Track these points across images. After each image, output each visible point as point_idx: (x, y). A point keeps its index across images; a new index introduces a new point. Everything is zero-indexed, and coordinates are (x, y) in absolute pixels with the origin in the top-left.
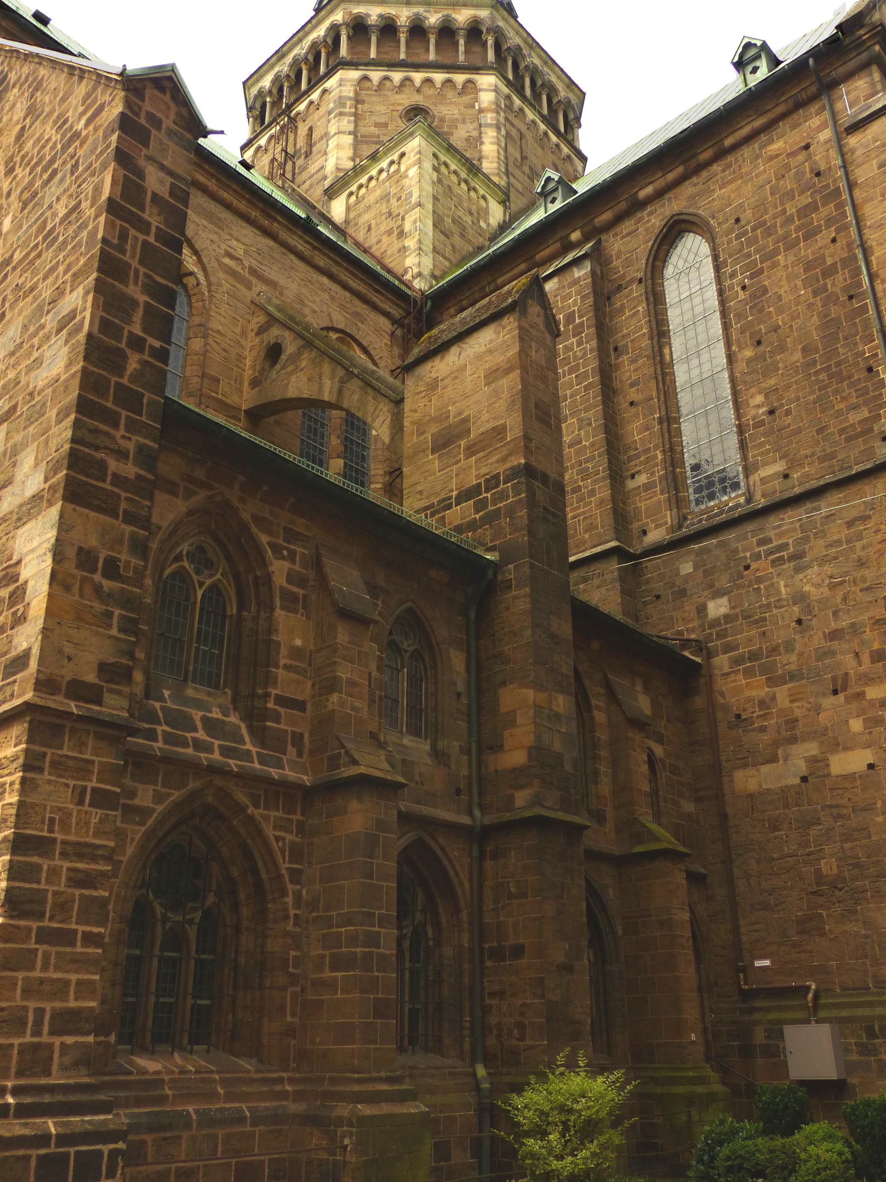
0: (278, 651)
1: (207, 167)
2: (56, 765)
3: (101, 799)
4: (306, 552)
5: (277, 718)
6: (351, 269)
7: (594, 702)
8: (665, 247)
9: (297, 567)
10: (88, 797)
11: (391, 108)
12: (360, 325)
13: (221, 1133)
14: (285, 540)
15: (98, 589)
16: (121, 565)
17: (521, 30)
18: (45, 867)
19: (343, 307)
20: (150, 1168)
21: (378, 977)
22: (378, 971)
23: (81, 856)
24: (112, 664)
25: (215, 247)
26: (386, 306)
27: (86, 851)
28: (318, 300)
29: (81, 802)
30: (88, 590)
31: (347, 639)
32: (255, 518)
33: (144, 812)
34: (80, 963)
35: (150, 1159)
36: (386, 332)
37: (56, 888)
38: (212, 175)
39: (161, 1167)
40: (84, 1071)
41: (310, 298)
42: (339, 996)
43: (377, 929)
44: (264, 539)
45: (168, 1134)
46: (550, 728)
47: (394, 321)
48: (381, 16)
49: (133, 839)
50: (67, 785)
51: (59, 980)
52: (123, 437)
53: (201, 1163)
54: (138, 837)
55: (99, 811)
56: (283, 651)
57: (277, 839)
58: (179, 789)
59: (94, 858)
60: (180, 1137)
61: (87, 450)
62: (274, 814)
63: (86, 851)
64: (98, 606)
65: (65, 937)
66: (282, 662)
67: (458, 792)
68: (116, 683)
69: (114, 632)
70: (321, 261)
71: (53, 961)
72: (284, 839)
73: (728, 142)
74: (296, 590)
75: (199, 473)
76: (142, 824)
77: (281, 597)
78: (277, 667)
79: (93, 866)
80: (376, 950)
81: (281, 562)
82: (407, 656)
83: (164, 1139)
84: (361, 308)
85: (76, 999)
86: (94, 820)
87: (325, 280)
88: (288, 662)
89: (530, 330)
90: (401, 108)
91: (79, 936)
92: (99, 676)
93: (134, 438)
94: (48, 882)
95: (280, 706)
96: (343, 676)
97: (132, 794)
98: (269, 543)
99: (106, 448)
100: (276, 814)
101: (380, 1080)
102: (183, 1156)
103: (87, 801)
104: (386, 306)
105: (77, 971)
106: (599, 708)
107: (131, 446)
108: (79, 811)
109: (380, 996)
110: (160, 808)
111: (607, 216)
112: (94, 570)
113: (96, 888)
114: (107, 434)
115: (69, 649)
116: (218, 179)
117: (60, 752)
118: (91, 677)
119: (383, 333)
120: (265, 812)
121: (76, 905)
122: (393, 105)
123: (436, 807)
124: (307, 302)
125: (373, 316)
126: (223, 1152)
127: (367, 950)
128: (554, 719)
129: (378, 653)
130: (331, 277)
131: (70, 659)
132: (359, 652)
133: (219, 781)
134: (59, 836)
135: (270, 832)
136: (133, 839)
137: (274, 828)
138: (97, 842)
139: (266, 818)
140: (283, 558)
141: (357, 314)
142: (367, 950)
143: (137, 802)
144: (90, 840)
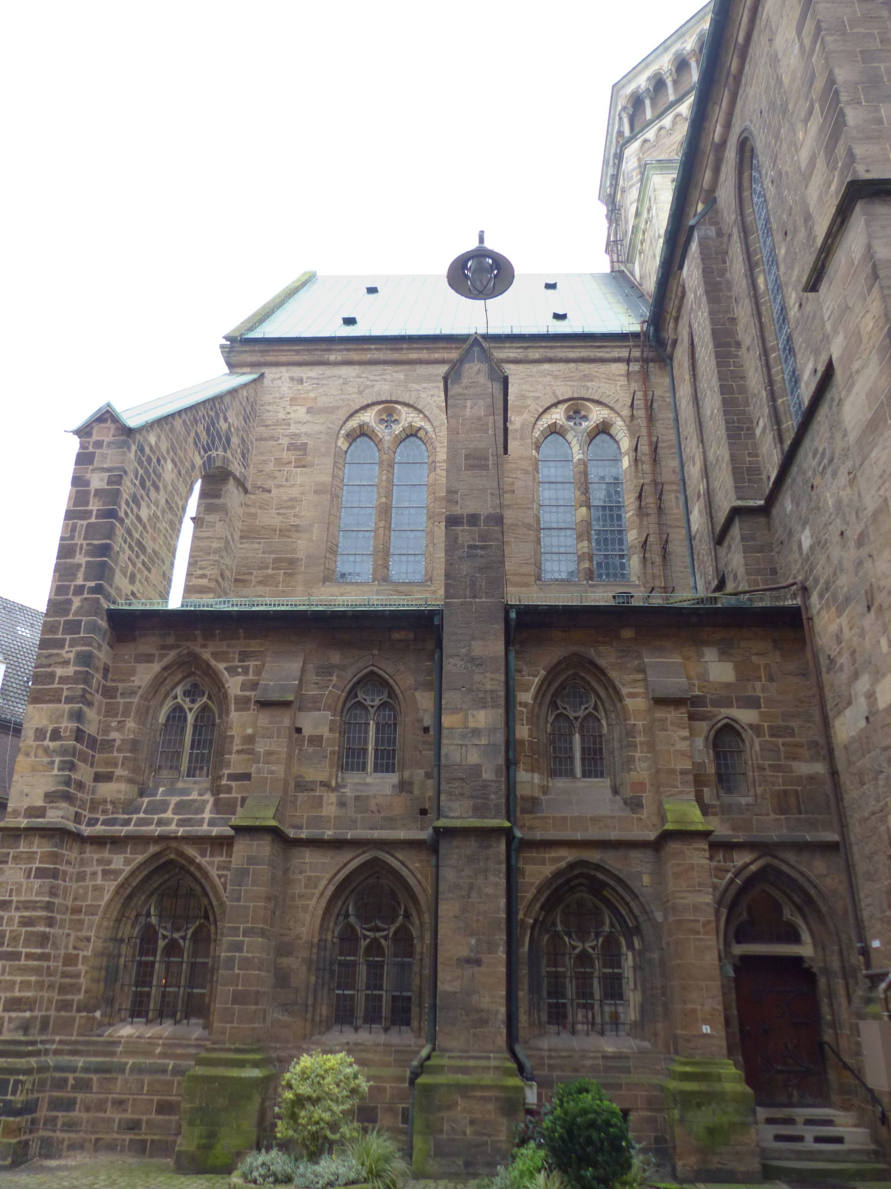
0: (231, 743)
1: (415, 346)
2: (15, 858)
3: (41, 873)
4: (259, 663)
5: (229, 790)
6: (566, 344)
7: (624, 691)
8: (746, 175)
9: (251, 677)
10: (33, 873)
11: (668, 151)
12: (589, 384)
13: (147, 1079)
14: (240, 661)
15: (46, 750)
16: (62, 730)
17: (680, 32)
18: (6, 918)
19: (566, 379)
20: (94, 1096)
21: (239, 974)
22: (239, 969)
23: (26, 908)
24: (53, 792)
25: (435, 398)
26: (615, 354)
27: (30, 905)
28: (540, 387)
29: (29, 877)
30: (40, 752)
31: (267, 721)
32: (215, 655)
33: (117, 873)
34: (23, 970)
35: (94, 1090)
36: (622, 375)
37: (12, 928)
38: (421, 349)
39: (102, 1096)
40: (21, 1032)
41: (532, 389)
42: (231, 989)
43: (241, 938)
44: (221, 666)
45: (108, 1076)
46: (462, 745)
47: (628, 361)
48: (649, 79)
49: (108, 890)
50: (21, 869)
51: (10, 981)
52: (67, 652)
53: (131, 1097)
54: (112, 889)
55: (40, 881)
56: (237, 741)
57: (220, 877)
58: (142, 854)
59: (35, 909)
60: (116, 1079)
61: (43, 670)
62: (217, 859)
63: (30, 905)
64: (46, 760)
65: (15, 956)
66: (235, 749)
67: (423, 812)
68: (55, 802)
69: (55, 772)
70: (535, 354)
71: (7, 969)
72: (226, 876)
73: (741, 39)
74: (248, 693)
75: (170, 641)
76: (115, 880)
77: (236, 703)
78: (231, 753)
79: (34, 914)
80: (237, 954)
81: (236, 678)
82: (372, 711)
83: (106, 1079)
84: (585, 368)
85: (20, 991)
86: (36, 886)
87: (547, 366)
88: (240, 748)
89: (465, 391)
90: (675, 147)
91: (23, 955)
92: (44, 802)
93: (74, 650)
94: (7, 925)
95: (232, 780)
96: (262, 750)
97: (109, 862)
98: (226, 669)
99: (56, 663)
100: (221, 859)
101: (229, 1050)
102: (118, 1090)
103: (32, 875)
104: (615, 354)
105: (21, 975)
106: (632, 695)
107: (72, 656)
108: (28, 883)
109: (240, 988)
110: (128, 869)
111: (708, 175)
112: (44, 739)
113: (34, 926)
114: (57, 655)
115: (26, 790)
116: (427, 349)
117: (18, 850)
118: (40, 803)
119: (617, 378)
120: (211, 859)
121: (22, 937)
122: (669, 147)
123: (395, 829)
124: (528, 394)
125: (604, 368)
126: (148, 1091)
127: (230, 954)
128: (470, 735)
129: (330, 718)
130: (550, 361)
131: (27, 795)
132: (278, 728)
133: (174, 844)
134: (14, 898)
135: (214, 873)
136: (108, 890)
137: (218, 869)
138: (37, 899)
139: (211, 864)
140: (238, 674)
141: (585, 376)
142: (230, 954)
143: (113, 866)
144: (34, 898)
